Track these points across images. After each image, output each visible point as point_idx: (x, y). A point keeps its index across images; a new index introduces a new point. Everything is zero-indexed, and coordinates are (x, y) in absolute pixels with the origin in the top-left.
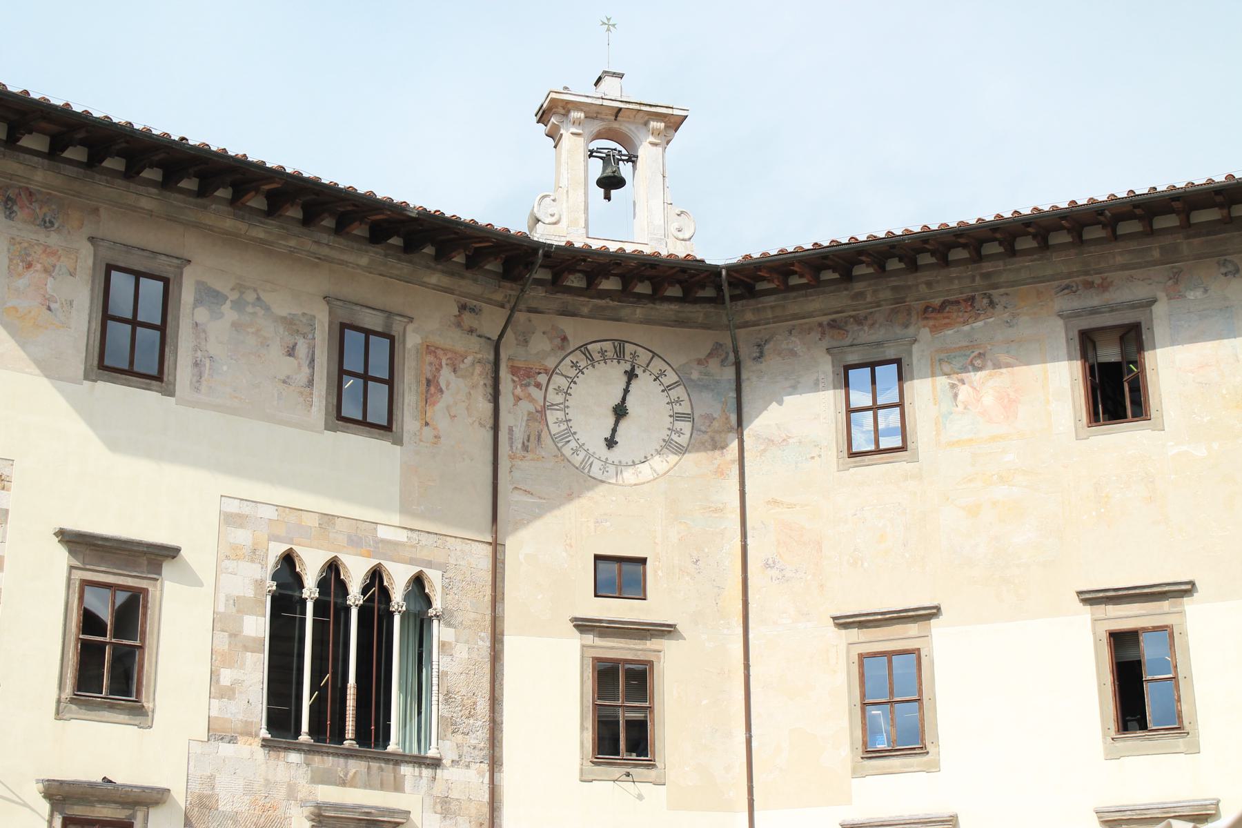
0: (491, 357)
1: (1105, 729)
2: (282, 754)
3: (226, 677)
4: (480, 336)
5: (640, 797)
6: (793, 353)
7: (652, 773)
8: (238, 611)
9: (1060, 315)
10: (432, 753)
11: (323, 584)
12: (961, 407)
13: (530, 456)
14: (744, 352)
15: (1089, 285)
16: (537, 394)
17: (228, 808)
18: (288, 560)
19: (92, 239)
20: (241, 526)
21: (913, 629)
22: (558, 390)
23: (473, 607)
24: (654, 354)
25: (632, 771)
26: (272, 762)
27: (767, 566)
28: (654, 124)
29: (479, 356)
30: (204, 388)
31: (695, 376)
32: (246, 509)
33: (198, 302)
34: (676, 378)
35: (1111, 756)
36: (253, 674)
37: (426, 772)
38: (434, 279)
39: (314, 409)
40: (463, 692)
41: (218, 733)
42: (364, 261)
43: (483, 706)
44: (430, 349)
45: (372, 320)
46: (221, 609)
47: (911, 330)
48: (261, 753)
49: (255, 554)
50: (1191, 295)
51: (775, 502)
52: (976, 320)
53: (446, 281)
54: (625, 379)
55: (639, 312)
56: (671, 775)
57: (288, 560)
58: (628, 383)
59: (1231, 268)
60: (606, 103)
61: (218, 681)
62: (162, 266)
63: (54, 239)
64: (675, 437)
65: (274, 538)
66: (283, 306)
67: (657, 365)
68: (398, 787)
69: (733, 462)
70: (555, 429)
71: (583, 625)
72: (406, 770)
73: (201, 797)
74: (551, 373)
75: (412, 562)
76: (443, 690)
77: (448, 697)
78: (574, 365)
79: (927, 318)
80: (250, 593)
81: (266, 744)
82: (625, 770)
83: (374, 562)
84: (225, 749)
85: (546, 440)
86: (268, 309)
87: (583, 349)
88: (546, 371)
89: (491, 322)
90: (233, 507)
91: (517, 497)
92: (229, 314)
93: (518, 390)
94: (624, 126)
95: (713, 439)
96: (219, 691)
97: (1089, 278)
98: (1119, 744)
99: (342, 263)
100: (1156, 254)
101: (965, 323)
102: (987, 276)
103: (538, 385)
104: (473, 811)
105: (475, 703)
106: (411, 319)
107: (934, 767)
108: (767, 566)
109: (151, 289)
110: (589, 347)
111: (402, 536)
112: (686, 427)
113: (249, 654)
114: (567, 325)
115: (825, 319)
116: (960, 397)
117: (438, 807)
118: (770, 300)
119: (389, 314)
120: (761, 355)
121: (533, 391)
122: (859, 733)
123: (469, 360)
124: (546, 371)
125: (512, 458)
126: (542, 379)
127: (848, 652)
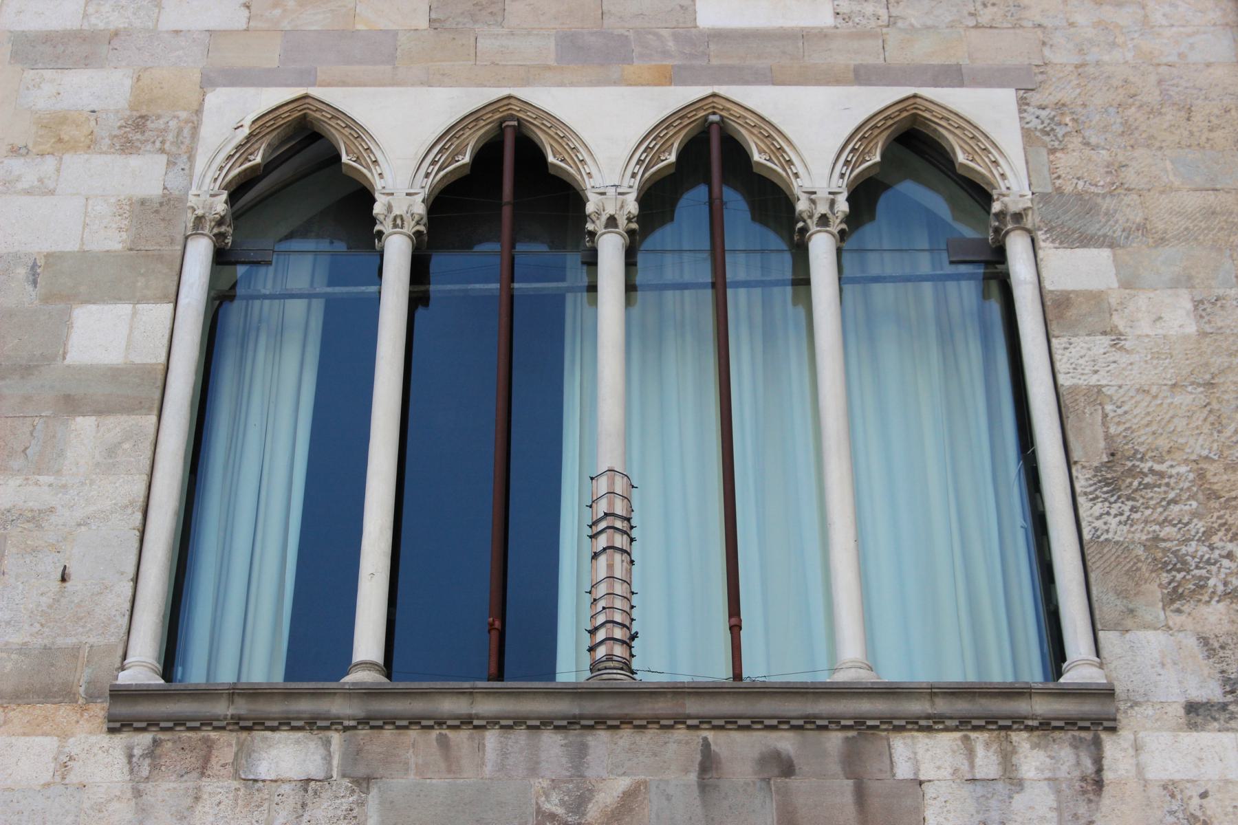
2: (226, 744)
8: (46, 299)
20: (86, 62)
26: (166, 790)
40: (1199, 446)
48: (104, 759)
76: (1091, 450)
80: (111, 239)
113: (85, 424)
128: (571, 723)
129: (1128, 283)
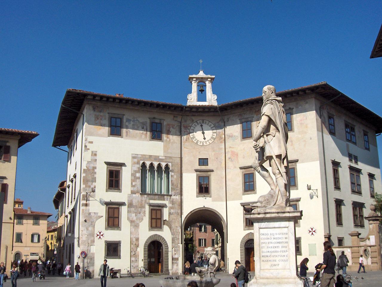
0: (180, 124)
3: (134, 184)
4: (178, 121)
6: (233, 120)
7: (209, 195)
10: (170, 194)
11: (149, 167)
13: (187, 142)
14: (226, 120)
16: (188, 131)
17: (135, 205)
18: (144, 163)
19: (108, 113)
20: (135, 159)
22: (192, 130)
23: (177, 169)
25: (205, 195)
27: (229, 159)
28: (209, 79)
29: (177, 125)
32: (136, 156)
33: (126, 121)
34: (213, 126)
36: (138, 183)
37: (169, 197)
38: (169, 112)
39: (147, 137)
41: (133, 192)
42: (155, 111)
43: (179, 186)
45: (157, 121)
46: (132, 172)
47: (253, 116)
48: (140, 196)
49: (138, 163)
50: (300, 107)
51: (230, 147)
53: (171, 112)
55: (206, 114)
56: (212, 196)
57: (144, 163)
58: (202, 127)
59: (306, 102)
60: (200, 77)
61: (132, 184)
62: (120, 116)
63: (102, 114)
65: (142, 160)
66: (141, 120)
67: (210, 124)
68: (164, 200)
70: (191, 137)
71: (196, 171)
72: (166, 197)
73: (130, 203)
74: (191, 127)
75: (166, 162)
77: (173, 184)
78: (195, 125)
80: (137, 170)
81: (141, 194)
83: (159, 163)
84: (134, 195)
86: (138, 121)
87: (196, 122)
88: (190, 126)
90: (134, 156)
91: (185, 149)
92: (132, 123)
93: (185, 130)
94: (204, 80)
95: (220, 136)
96: (133, 186)
99: (151, 111)
103: (188, 129)
104: (178, 203)
105: (178, 185)
106: (164, 120)
108: (229, 159)
109: (118, 120)
111: (164, 158)
112: (215, 134)
114: (193, 118)
115: (239, 114)
117: (172, 203)
118: (229, 111)
119: (160, 120)
120: (228, 120)
123: (175, 126)
124: (190, 126)
125: (184, 142)
126: (189, 128)
129: (174, 175)
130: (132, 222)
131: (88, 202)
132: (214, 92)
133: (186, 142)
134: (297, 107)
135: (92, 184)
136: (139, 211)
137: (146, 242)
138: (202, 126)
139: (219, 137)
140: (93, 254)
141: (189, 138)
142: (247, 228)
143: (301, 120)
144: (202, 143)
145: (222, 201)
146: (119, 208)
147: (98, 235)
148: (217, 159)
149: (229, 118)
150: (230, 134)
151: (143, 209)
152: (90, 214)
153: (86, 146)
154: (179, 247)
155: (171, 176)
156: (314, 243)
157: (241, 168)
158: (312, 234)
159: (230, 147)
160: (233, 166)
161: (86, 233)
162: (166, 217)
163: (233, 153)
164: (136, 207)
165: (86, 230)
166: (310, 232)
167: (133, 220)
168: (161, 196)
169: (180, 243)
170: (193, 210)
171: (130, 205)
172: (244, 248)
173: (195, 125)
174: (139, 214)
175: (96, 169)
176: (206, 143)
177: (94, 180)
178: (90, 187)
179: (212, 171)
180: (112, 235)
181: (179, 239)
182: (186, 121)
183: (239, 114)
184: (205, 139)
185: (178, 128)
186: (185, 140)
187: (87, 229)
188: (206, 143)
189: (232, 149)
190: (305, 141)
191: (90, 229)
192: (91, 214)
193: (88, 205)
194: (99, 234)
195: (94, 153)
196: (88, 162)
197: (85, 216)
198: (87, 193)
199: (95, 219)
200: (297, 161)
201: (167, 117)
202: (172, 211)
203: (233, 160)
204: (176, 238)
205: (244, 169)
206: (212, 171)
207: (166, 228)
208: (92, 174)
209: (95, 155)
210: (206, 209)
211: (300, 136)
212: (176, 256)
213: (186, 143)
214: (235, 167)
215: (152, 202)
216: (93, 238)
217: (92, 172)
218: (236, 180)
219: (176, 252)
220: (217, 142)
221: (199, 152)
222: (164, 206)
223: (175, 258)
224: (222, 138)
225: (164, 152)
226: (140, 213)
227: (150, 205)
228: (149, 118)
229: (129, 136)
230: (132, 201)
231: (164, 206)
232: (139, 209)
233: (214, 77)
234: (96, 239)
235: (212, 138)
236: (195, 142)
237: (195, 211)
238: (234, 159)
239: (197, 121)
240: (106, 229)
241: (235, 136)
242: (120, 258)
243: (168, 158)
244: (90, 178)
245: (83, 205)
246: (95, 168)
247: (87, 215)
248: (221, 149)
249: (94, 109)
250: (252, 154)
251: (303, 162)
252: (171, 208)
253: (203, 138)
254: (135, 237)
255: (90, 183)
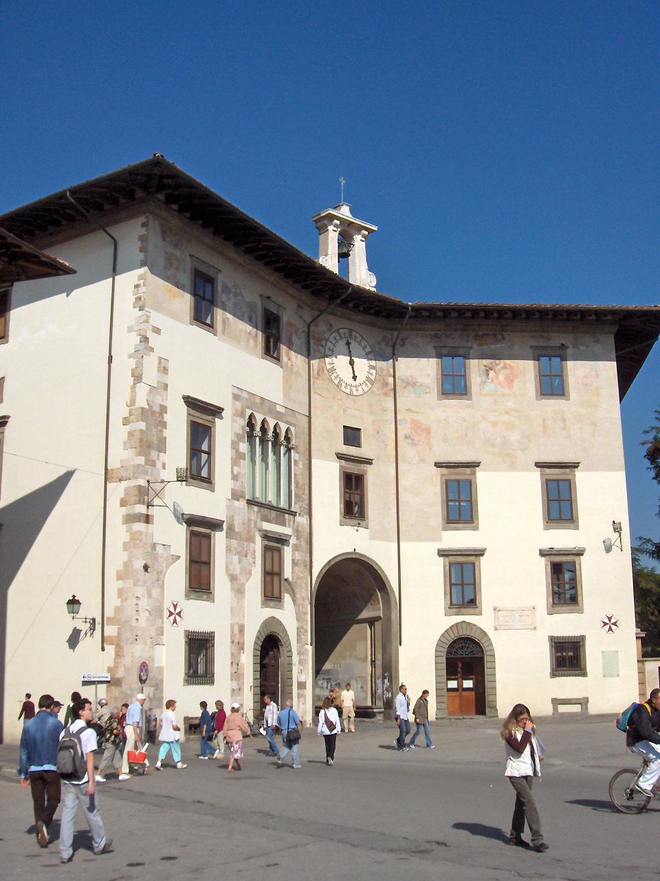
0: (307, 330)
1: (544, 519)
5: (357, 531)
9: (531, 347)
10: (293, 509)
12: (490, 380)
13: (320, 378)
15: (543, 337)
19: (191, 256)
21: (468, 471)
22: (329, 349)
24: (363, 338)
27: (406, 437)
30: (226, 333)
31: (377, 349)
35: (546, 528)
37: (292, 517)
41: (236, 496)
42: (272, 279)
44: (290, 324)
45: (273, 309)
46: (233, 439)
47: (469, 345)
49: (242, 414)
50: (583, 348)
51: (409, 410)
52: (497, 343)
54: (347, 347)
56: (371, 524)
57: (251, 416)
63: (178, 253)
64: (370, 376)
67: (364, 343)
69: (391, 390)
70: (328, 367)
71: (340, 456)
72: (287, 516)
74: (327, 341)
75: (286, 422)
77: (297, 486)
78: (335, 338)
79: (476, 340)
80: (241, 432)
82: (357, 522)
84: (236, 503)
85: (326, 371)
89: (308, 315)
90: (236, 391)
92: (233, 299)
93: (315, 347)
94: (352, 231)
96: (235, 477)
97: (543, 334)
98: (549, 524)
100: (570, 328)
101: (492, 344)
102: (503, 326)
103: (322, 346)
107: (476, 528)
108: (406, 437)
110: (340, 330)
111: (282, 410)
112: (374, 372)
114: (332, 319)
116: (490, 376)
119: (279, 306)
120: (404, 344)
121: (322, 349)
122: (445, 513)
126: (324, 343)
127: (441, 478)
128: (270, 509)
130: (233, 578)
131: (152, 511)
132: (372, 267)
133: (317, 378)
134: (575, 347)
135: (159, 455)
136: (245, 548)
137: (258, 638)
138: (348, 344)
139: (382, 382)
140: (160, 669)
141: (323, 369)
142: (455, 610)
143: (585, 377)
144: (349, 387)
145: (388, 540)
146: (208, 537)
147: (171, 614)
148: (378, 433)
149: (406, 339)
150: (410, 379)
151: (252, 545)
152: (154, 546)
153: (145, 339)
154: (307, 650)
155: (295, 461)
156: (614, 649)
157: (438, 465)
158: (610, 629)
159: (409, 410)
160: (417, 458)
161: (148, 608)
162: (288, 573)
163: (417, 426)
164: (240, 537)
165: (146, 596)
166: (615, 624)
167: (235, 573)
168: (282, 513)
169: (309, 642)
170: (334, 558)
171: (231, 533)
172: (444, 660)
173: (335, 338)
174: (244, 559)
175: (166, 413)
176: (357, 390)
177: (161, 446)
178: (153, 464)
179: (368, 462)
180: (199, 615)
181: (307, 632)
182: (317, 325)
183: (433, 333)
184: (355, 378)
185: (304, 341)
186: (316, 372)
187: (150, 595)
188: (357, 390)
189: (416, 417)
190: (593, 424)
191: (155, 592)
192: (157, 549)
193: (150, 518)
194: (172, 609)
195: (163, 365)
196: (153, 389)
197: (146, 552)
198: (148, 481)
199: (164, 565)
200: (575, 466)
201: (300, 302)
202: (298, 556)
203: (416, 442)
204: (302, 628)
205: (447, 467)
206: (368, 462)
207: (287, 598)
208: (159, 428)
209: (165, 370)
210: (358, 557)
211: (583, 412)
212: (302, 679)
213: (318, 381)
214: (423, 461)
215: (267, 526)
216: (160, 620)
217: (160, 422)
218: (427, 494)
219: (302, 668)
220: (377, 392)
221: (344, 411)
222: (282, 540)
223: (301, 682)
224: (387, 384)
225: (286, 395)
226: (246, 556)
227: (266, 536)
228: (261, 295)
229: (228, 333)
230: (233, 521)
231: (282, 540)
232: (245, 543)
233: (375, 228)
234: (168, 622)
235: (368, 378)
236: (336, 382)
237: (337, 560)
238: (419, 441)
239: (338, 330)
240: (187, 596)
241: (421, 385)
242: (212, 682)
243: (290, 413)
244: (155, 438)
245: (130, 519)
246: (164, 409)
247: (149, 550)
248: (385, 411)
249: (163, 232)
250: (466, 435)
251: (588, 469)
252: (296, 548)
253: (351, 371)
254: (237, 623)
255: (154, 454)
